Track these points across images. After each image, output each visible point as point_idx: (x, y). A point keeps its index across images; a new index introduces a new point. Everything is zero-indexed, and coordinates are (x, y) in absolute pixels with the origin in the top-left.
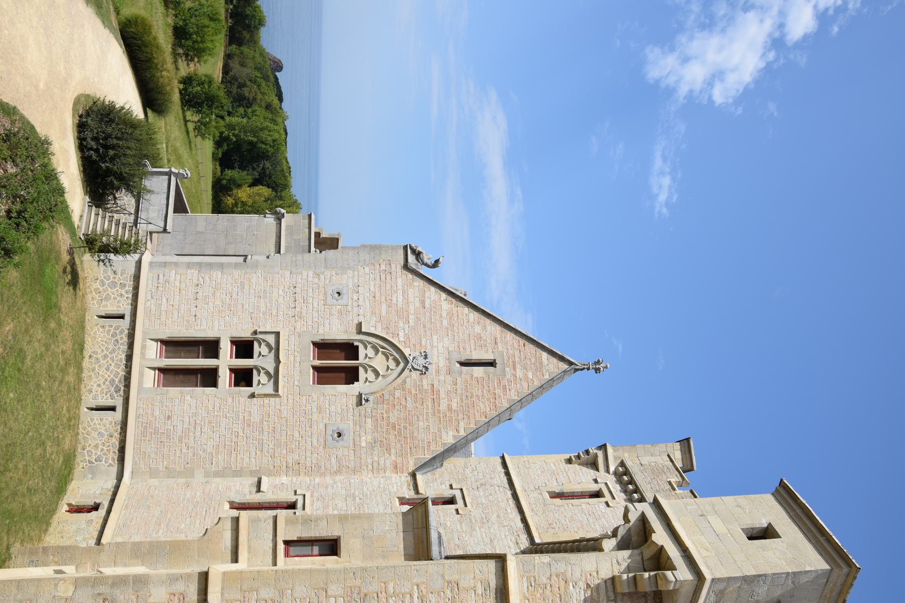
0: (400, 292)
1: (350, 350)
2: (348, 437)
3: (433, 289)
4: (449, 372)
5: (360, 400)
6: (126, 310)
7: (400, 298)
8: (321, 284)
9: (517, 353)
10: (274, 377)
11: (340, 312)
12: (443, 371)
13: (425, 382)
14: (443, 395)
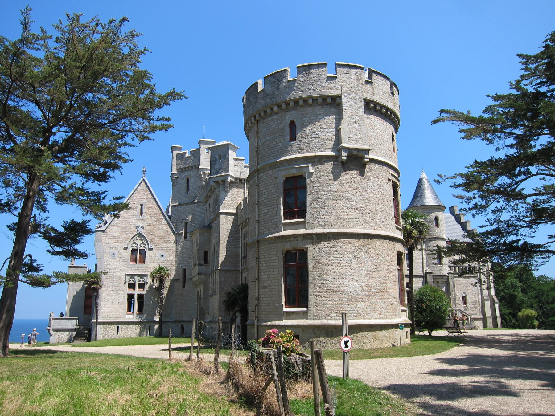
0: (113, 234)
1: (134, 251)
2: (163, 253)
3: (113, 222)
4: (144, 220)
5: (151, 249)
6: (116, 326)
7: (116, 234)
8: (109, 260)
9: (138, 197)
10: (142, 276)
11: (120, 254)
12: (143, 222)
13: (147, 228)
14: (151, 223)
